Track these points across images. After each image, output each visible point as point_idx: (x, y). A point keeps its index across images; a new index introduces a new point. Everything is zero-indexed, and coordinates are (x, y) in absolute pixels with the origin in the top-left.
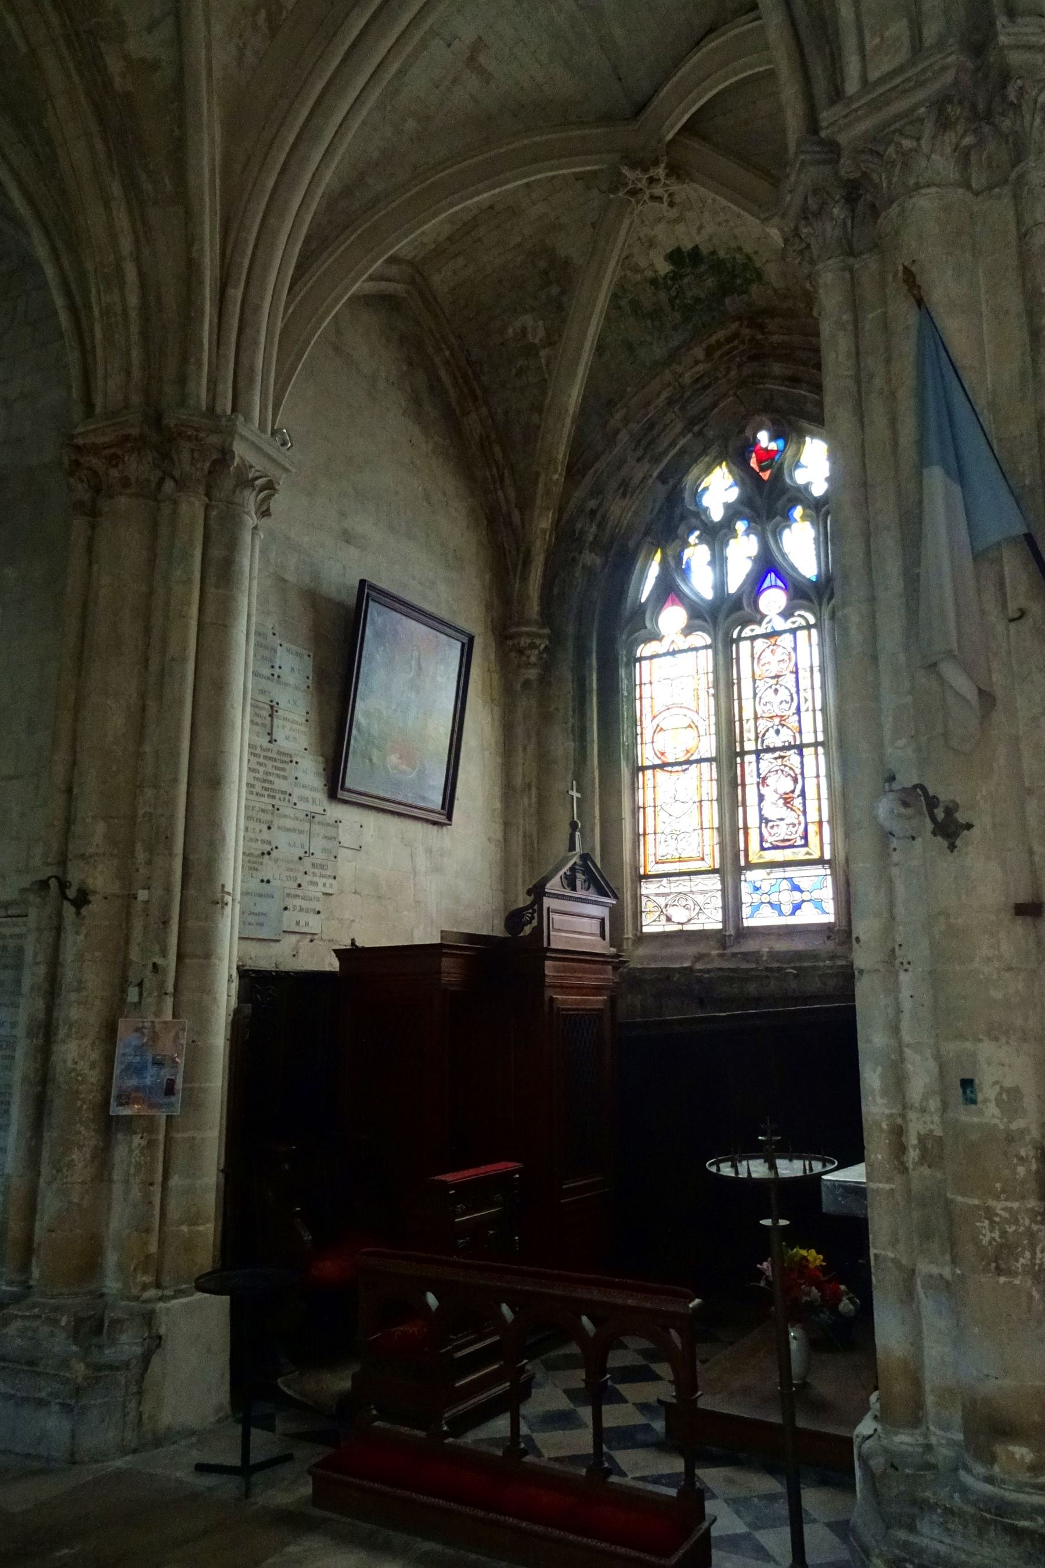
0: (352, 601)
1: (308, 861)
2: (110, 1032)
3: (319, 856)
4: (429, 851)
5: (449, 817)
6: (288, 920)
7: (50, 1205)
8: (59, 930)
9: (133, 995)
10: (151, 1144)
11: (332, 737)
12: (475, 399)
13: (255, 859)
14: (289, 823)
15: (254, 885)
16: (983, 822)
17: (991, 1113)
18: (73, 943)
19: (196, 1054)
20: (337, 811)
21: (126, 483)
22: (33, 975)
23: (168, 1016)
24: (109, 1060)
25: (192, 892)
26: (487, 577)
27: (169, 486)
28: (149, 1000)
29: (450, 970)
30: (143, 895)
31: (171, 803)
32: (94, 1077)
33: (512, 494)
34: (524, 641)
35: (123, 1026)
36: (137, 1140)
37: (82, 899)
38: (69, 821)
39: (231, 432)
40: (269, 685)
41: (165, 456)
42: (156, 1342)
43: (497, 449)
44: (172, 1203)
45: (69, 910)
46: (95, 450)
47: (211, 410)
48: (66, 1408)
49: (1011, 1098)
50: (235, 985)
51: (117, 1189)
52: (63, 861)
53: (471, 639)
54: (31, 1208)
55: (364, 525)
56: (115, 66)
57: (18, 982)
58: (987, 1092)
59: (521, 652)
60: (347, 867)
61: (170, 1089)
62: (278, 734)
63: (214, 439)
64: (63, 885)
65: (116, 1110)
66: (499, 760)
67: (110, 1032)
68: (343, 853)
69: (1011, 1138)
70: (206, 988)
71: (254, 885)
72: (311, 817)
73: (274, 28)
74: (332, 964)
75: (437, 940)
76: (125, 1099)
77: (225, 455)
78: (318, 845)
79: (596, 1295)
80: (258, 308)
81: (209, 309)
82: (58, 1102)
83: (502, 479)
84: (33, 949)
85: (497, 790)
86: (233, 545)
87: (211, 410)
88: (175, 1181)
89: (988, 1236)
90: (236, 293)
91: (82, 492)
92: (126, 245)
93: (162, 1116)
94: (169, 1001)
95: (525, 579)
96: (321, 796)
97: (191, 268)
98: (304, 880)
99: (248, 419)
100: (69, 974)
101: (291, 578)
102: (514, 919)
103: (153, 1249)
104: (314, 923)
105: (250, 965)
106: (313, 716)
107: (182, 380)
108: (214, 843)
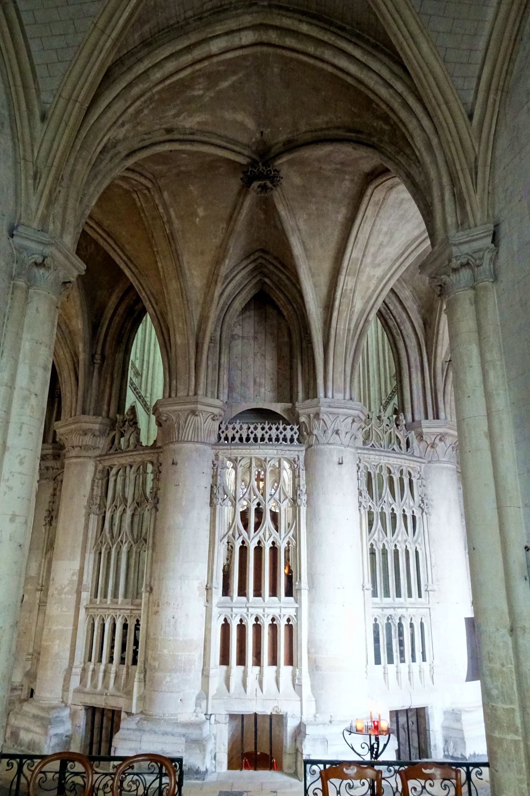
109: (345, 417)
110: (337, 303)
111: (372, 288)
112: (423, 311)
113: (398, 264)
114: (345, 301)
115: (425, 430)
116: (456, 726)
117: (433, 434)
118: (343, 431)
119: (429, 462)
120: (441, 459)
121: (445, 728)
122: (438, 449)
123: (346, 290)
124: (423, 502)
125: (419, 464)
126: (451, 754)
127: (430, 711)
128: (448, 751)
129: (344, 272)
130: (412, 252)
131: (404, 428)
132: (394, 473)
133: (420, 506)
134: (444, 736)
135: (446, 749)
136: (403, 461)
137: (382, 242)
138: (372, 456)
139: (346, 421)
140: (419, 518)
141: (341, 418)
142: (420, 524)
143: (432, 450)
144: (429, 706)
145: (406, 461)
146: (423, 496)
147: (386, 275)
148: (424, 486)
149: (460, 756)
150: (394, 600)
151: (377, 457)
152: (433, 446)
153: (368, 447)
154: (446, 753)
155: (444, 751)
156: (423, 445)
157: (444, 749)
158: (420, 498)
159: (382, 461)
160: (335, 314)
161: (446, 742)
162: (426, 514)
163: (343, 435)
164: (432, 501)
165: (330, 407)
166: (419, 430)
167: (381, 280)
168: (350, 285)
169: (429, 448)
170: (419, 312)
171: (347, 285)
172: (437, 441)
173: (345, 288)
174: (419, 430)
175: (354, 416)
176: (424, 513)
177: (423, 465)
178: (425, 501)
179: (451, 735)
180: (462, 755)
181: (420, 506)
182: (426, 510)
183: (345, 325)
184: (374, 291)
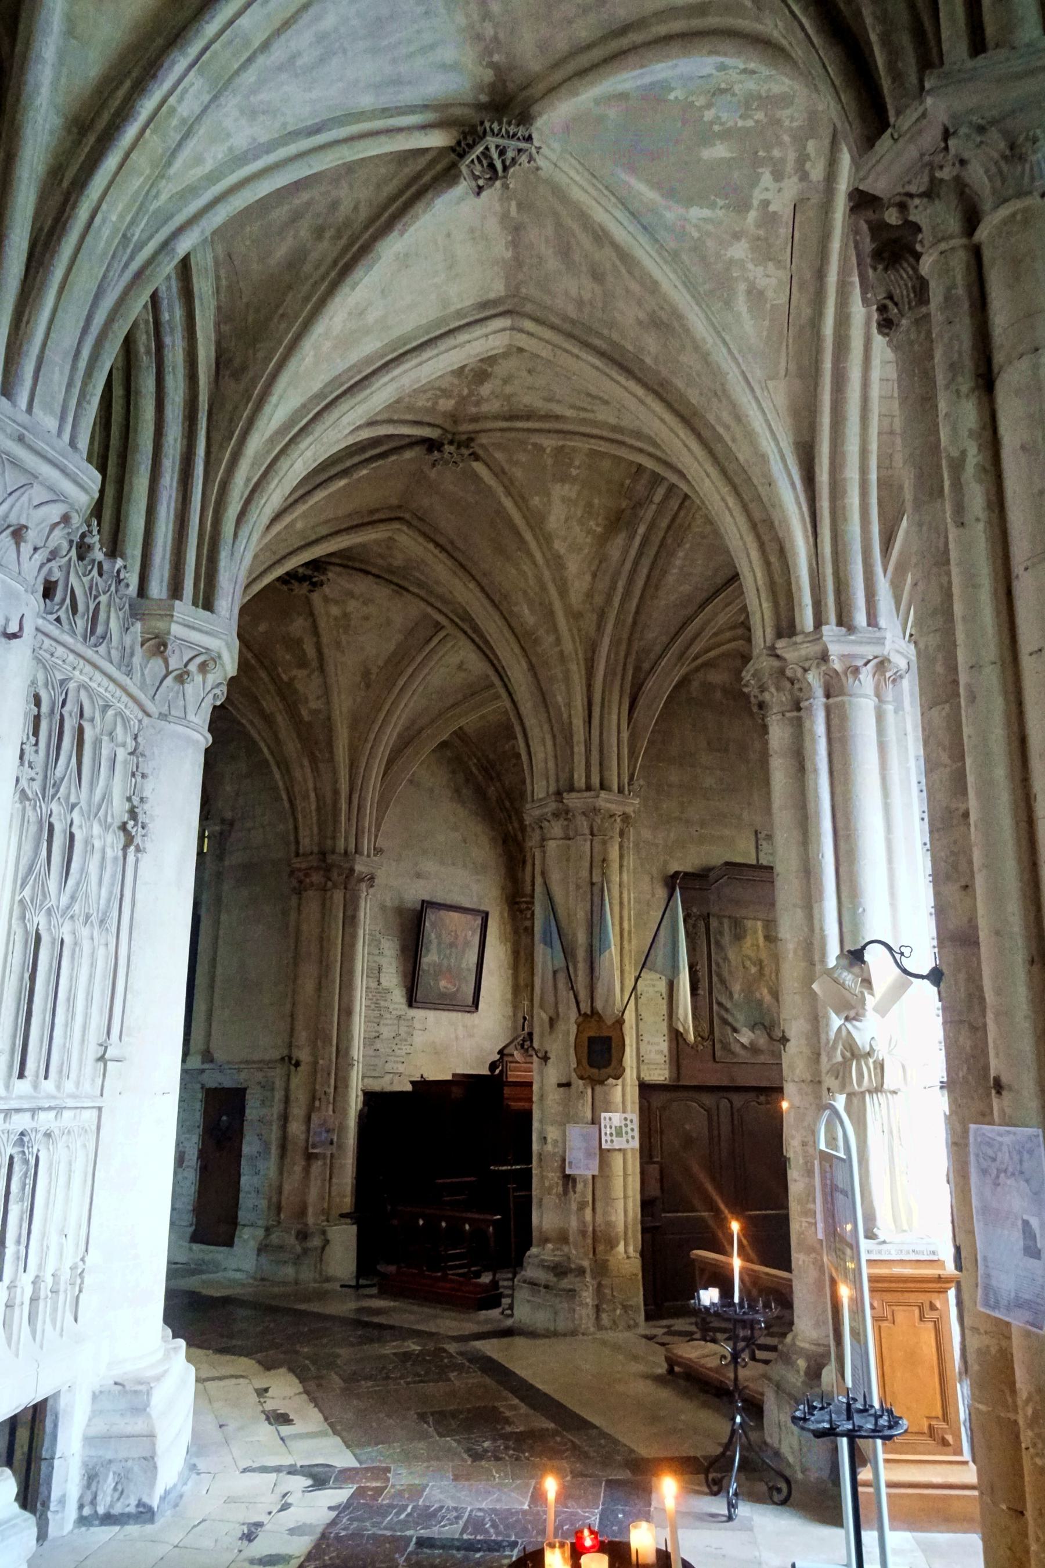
0: (419, 908)
1: (397, 1040)
2: (308, 1120)
3: (403, 1035)
4: (465, 1026)
5: (477, 1008)
6: (388, 1067)
7: (287, 1188)
8: (289, 1076)
9: (317, 1103)
10: (325, 1164)
11: (410, 977)
12: (492, 779)
13: (372, 1040)
14: (389, 1022)
15: (372, 1053)
16: (552, 1055)
17: (549, 1147)
18: (295, 1081)
19: (342, 1128)
20: (413, 1012)
21: (312, 884)
22: (279, 1095)
23: (331, 1112)
24: (308, 1130)
25: (340, 1060)
26: (503, 871)
27: (330, 884)
28: (323, 1107)
29: (457, 1092)
30: (321, 1062)
31: (332, 1023)
32: (303, 1137)
33: (516, 825)
34: (523, 906)
35: (314, 1117)
36: (320, 1163)
37: (297, 1064)
38: (292, 1030)
39: (354, 860)
40: (377, 958)
41: (328, 869)
42: (327, 1242)
43: (507, 804)
44: (334, 1188)
45: (293, 1068)
46: (299, 870)
47: (346, 852)
48: (295, 1264)
49: (556, 1141)
50: (361, 1098)
51: (313, 1183)
52: (290, 1045)
53: (487, 914)
54: (280, 1192)
55: (429, 866)
56: (304, 713)
57: (273, 1097)
58: (549, 1140)
59: (521, 912)
60: (419, 1039)
61: (332, 1143)
62: (382, 980)
63: (347, 865)
64: (290, 1058)
65: (311, 1151)
66: (510, 972)
67: (308, 1120)
68: (415, 1033)
69: (554, 1154)
70: (346, 1102)
71: (372, 1053)
72: (399, 1017)
73: (368, 686)
74: (409, 1088)
75: (449, 1077)
76: (314, 1146)
77: (352, 870)
78: (403, 1030)
79: (469, 1215)
80: (365, 799)
81: (344, 806)
82: (290, 1147)
83: (510, 817)
84: (279, 1083)
85: (509, 990)
86: (356, 909)
87: (346, 852)
88: (334, 1180)
89: (547, 1184)
90: (356, 796)
91: (295, 883)
92: (311, 785)
93: (328, 1153)
94: (331, 1107)
95: (523, 870)
96: (405, 1007)
97: (336, 792)
98: (396, 1048)
99: (362, 854)
100: (292, 1097)
101: (389, 904)
102: (493, 1066)
103: (326, 1205)
104: (401, 1068)
105: (370, 1088)
106: (401, 968)
107: (334, 838)
108: (350, 1040)
109: (47, 496)
110: (131, 132)
111: (209, 166)
112: (226, 328)
113: (292, 149)
114: (153, 141)
115: (176, 629)
116: (137, 1426)
117: (190, 644)
118: (32, 536)
119: (163, 717)
120: (191, 717)
121: (89, 1440)
122: (189, 688)
123: (173, 111)
124: (133, 814)
125: (140, 715)
126: (101, 1510)
127: (63, 1403)
128: (93, 1503)
129: (193, 50)
130: (337, 142)
131: (127, 606)
132: (92, 720)
133: (123, 827)
134: (85, 1465)
135: (88, 1497)
136: (119, 692)
137: (299, 54)
138: (60, 651)
139: (44, 509)
140: (116, 859)
141: (38, 494)
142: (114, 876)
143: (177, 687)
144: (64, 1388)
145: (125, 698)
146: (136, 800)
147: (256, 158)
148: (144, 776)
149: (132, 1509)
150: (36, 1086)
151: (71, 657)
152: (181, 678)
153: (49, 617)
154: (87, 1511)
155: (81, 1507)
156: (156, 665)
157: (81, 1497)
158: (127, 806)
159: (77, 673)
160: (111, 162)
161: (91, 1478)
162: (138, 850)
163: (26, 548)
164: (152, 817)
165: (21, 439)
166: (161, 625)
167: (240, 159)
168: (187, 107)
169: (170, 679)
170: (218, 325)
171: (181, 100)
172: (193, 667)
173: (172, 100)
174: (161, 625)
175: (72, 506)
176: (132, 848)
177: (146, 721)
178: (141, 818)
179: (109, 1455)
180: (140, 1504)
181: (123, 827)
182: (138, 840)
183: (121, 217)
184: (212, 178)
